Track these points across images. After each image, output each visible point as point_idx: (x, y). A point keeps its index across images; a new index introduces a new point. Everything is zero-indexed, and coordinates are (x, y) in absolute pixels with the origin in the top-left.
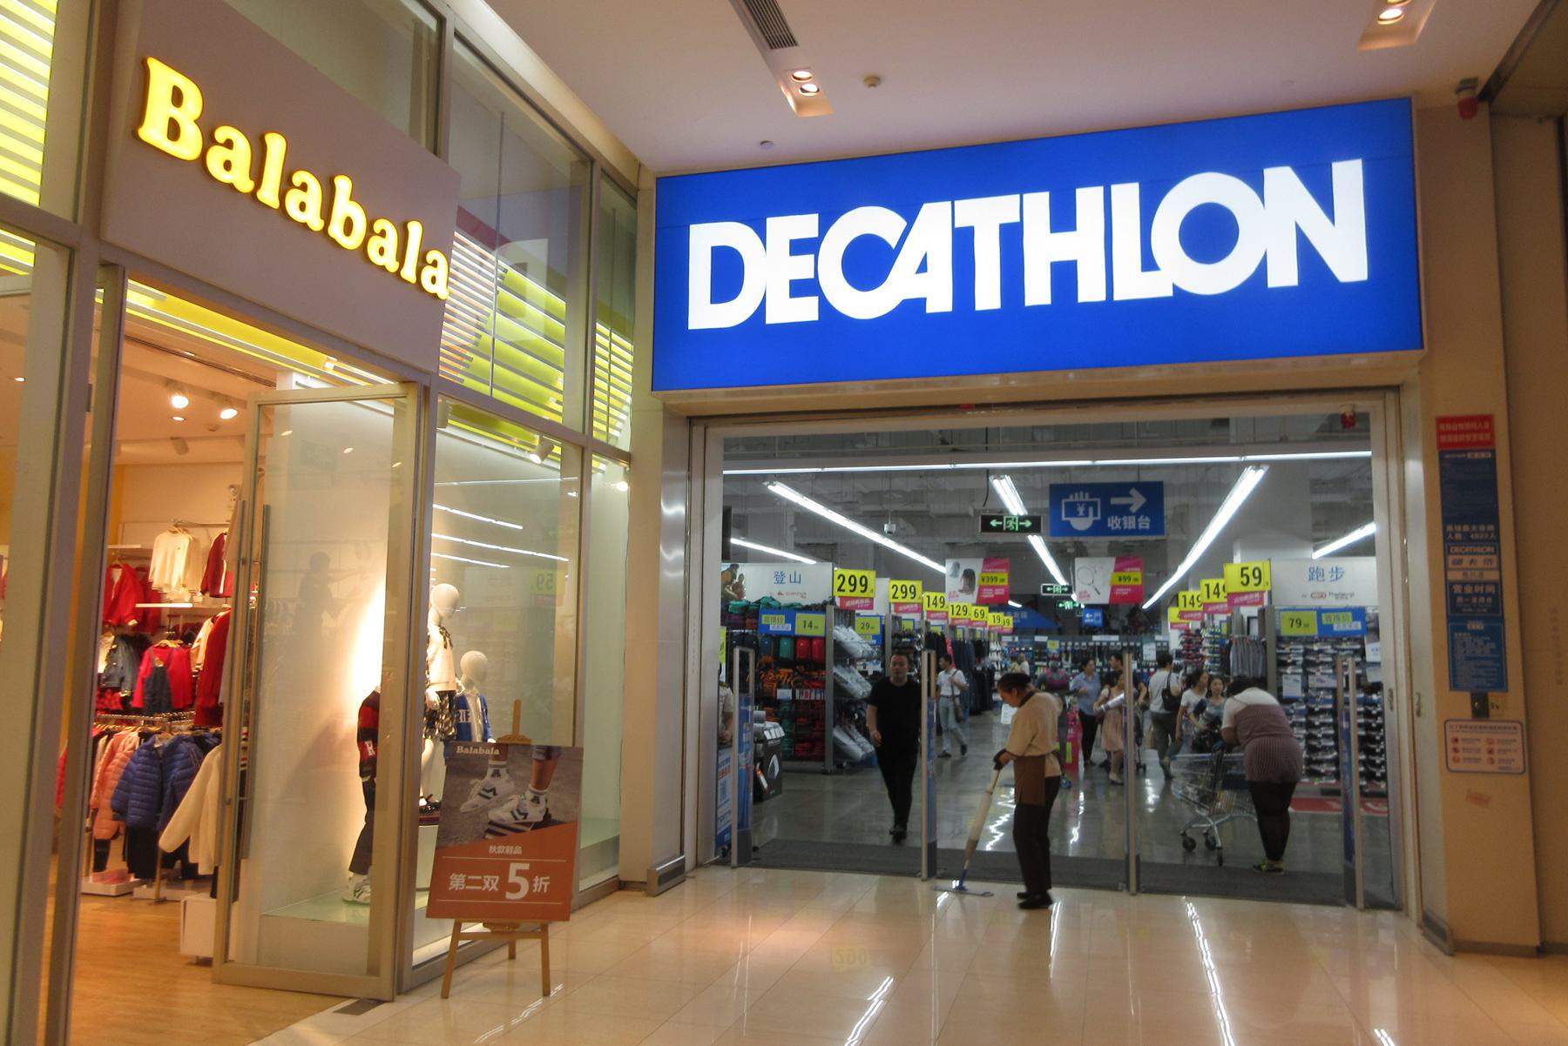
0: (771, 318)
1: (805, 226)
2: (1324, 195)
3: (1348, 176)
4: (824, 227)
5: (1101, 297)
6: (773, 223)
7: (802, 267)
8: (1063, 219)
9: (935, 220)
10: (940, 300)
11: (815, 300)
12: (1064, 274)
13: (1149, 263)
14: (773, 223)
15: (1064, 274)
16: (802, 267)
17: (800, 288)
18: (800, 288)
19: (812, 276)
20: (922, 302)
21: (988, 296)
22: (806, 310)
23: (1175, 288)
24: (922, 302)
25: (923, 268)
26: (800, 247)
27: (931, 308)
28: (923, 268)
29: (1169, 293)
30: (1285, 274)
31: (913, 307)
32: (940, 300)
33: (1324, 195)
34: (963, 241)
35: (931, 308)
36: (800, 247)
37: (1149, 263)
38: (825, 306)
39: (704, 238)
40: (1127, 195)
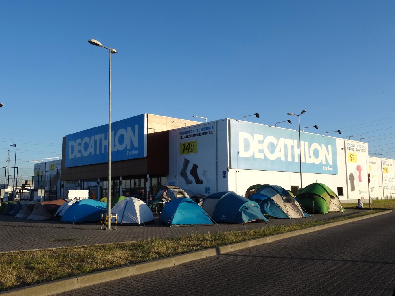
5: (304, 162)
10: (283, 159)
11: (263, 154)
13: (310, 157)
19: (262, 149)
20: (280, 158)
23: (313, 162)
24: (280, 158)
25: (280, 151)
26: (261, 142)
28: (280, 151)
29: (312, 163)
30: (324, 163)
31: (279, 158)
32: (283, 159)
36: (261, 142)
37: (310, 157)
38: (265, 156)
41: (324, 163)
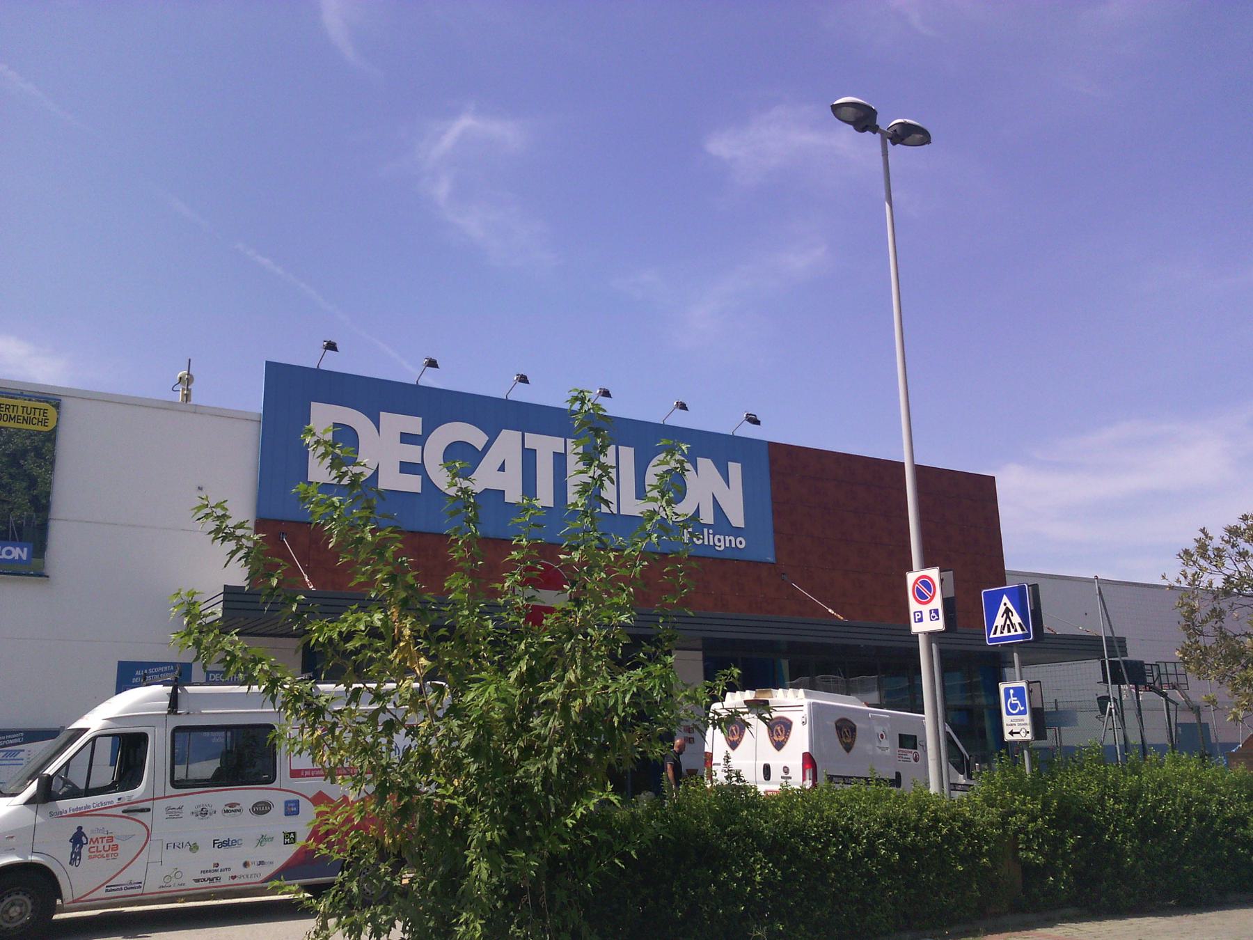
0: (384, 484)
1: (414, 425)
2: (23, 552)
3: (735, 469)
4: (428, 429)
6: (383, 416)
7: (411, 454)
8: (589, 458)
9: (509, 443)
10: (514, 495)
12: (592, 492)
13: (641, 493)
14: (383, 416)
15: (592, 492)
16: (411, 454)
17: (406, 468)
18: (407, 468)
20: (502, 493)
21: (545, 497)
22: (412, 484)
24: (502, 493)
25: (502, 468)
26: (406, 438)
27: (509, 499)
28: (502, 468)
30: (707, 517)
33: (23, 552)
34: (529, 457)
35: (509, 499)
36: (406, 438)
38: (427, 481)
39: (324, 417)
40: (628, 454)
41: (707, 517)
